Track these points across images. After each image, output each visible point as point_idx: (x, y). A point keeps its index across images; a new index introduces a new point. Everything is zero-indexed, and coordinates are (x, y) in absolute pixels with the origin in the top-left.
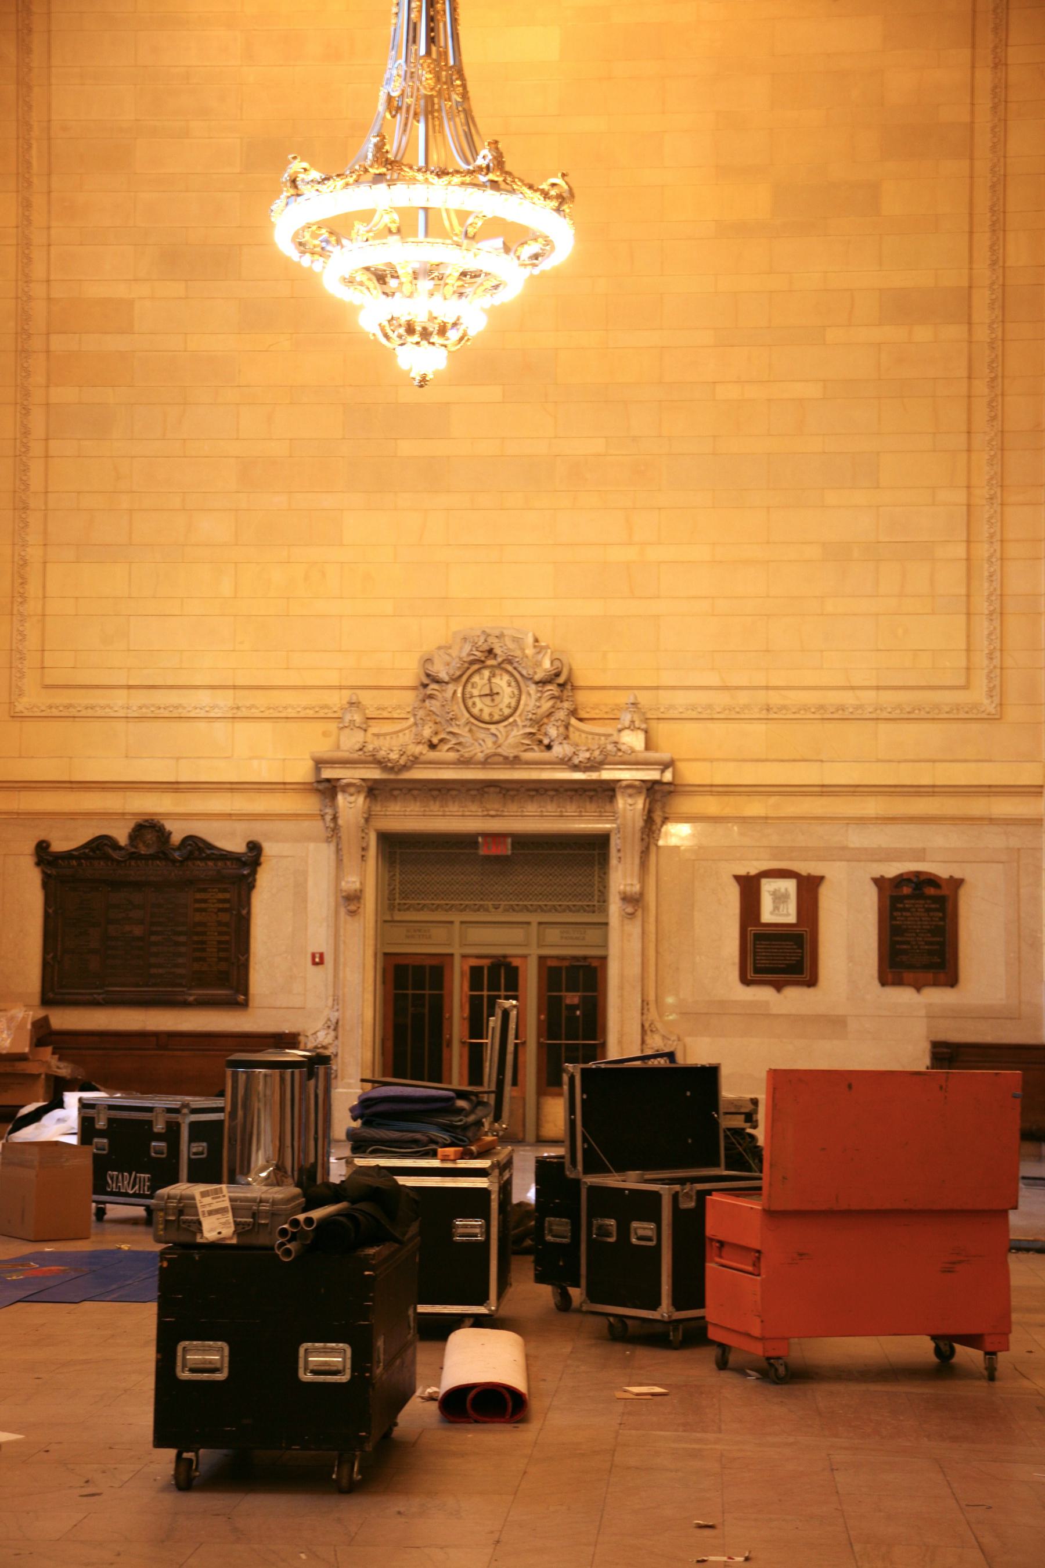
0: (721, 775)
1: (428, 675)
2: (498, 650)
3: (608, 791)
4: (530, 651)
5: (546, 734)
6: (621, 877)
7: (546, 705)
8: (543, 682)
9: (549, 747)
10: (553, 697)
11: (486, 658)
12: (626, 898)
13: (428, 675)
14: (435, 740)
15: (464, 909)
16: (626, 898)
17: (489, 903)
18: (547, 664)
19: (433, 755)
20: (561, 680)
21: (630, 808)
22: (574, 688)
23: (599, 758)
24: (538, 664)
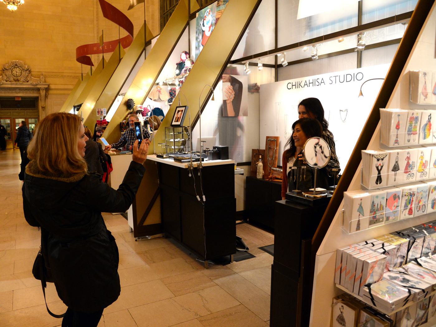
0: (57, 87)
1: (4, 68)
2: (18, 64)
3: (39, 90)
4: (24, 65)
5: (27, 79)
6: (41, 104)
7: (27, 74)
8: (26, 70)
9: (28, 82)
10: (28, 73)
11: (16, 66)
12: (43, 107)
13: (4, 68)
14: (7, 80)
15: (13, 110)
16: (43, 107)
17: (17, 109)
18: (26, 67)
19: (7, 83)
20: (29, 70)
21: (43, 93)
22: (31, 72)
23: (37, 83)
24: (25, 67)
